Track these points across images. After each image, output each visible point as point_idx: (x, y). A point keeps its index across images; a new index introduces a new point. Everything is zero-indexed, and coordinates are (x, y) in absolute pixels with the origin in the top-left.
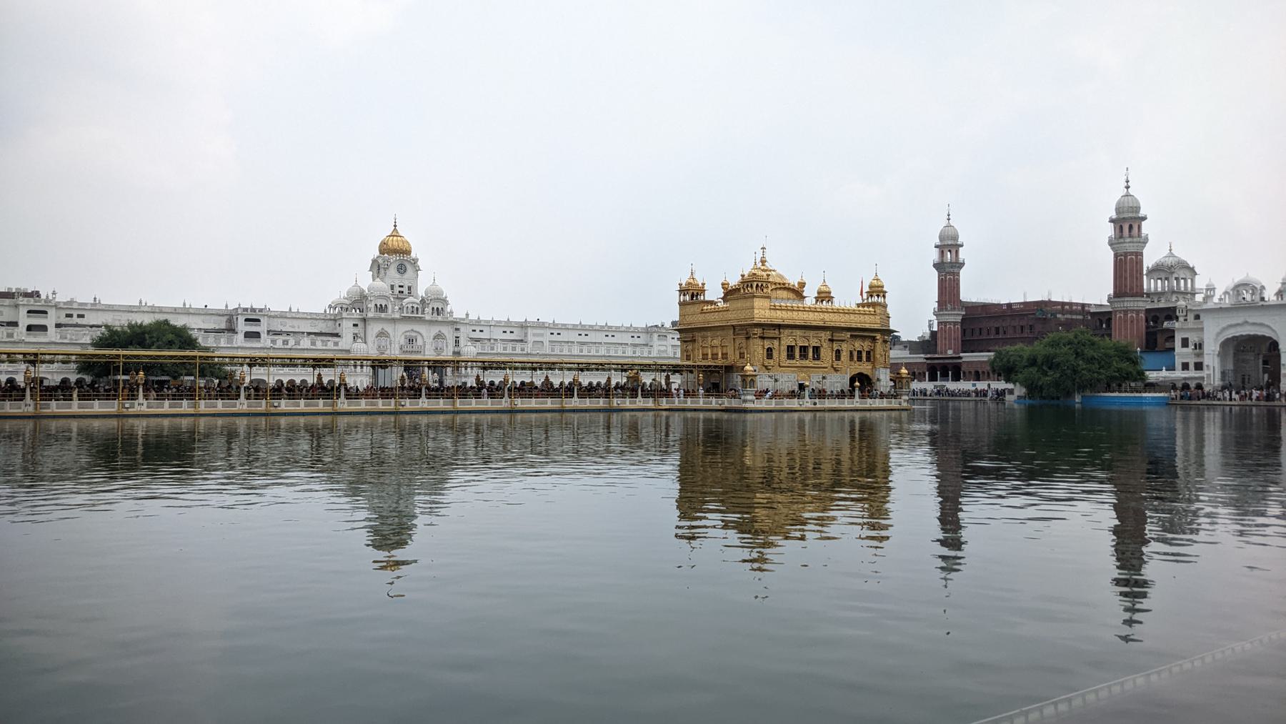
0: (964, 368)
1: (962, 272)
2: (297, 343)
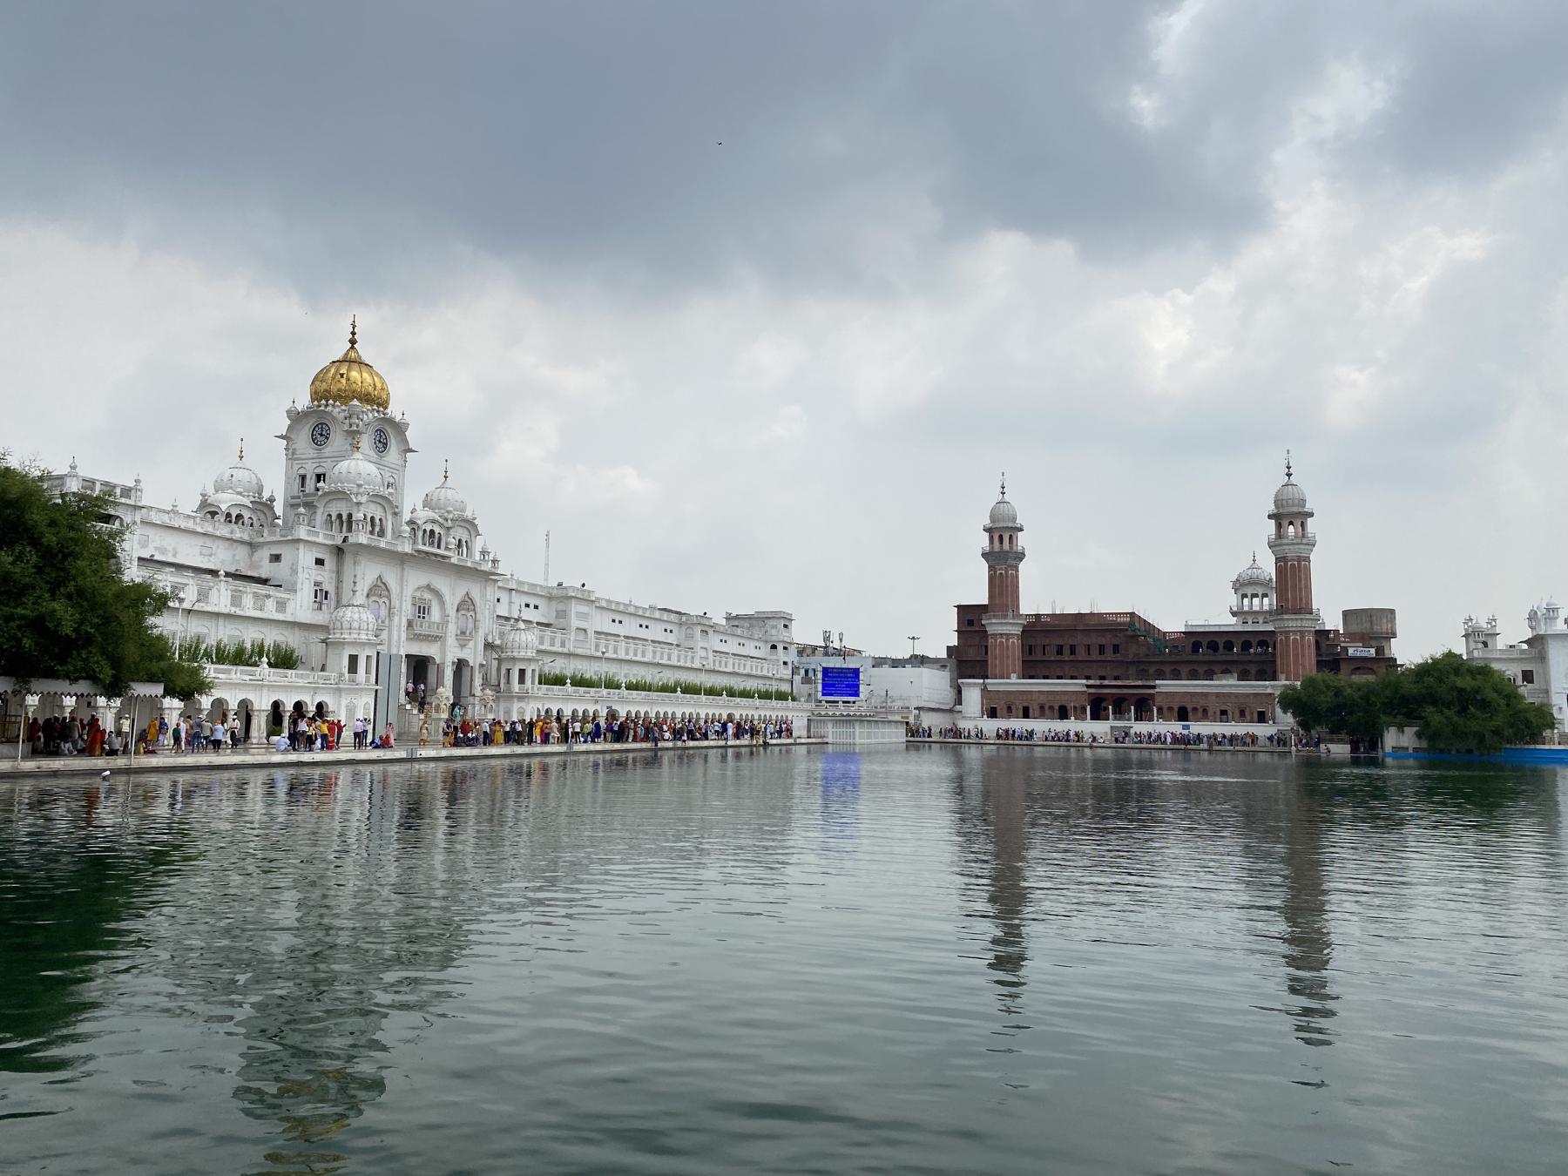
0: (1158, 700)
1: (1021, 566)
2: (203, 596)
